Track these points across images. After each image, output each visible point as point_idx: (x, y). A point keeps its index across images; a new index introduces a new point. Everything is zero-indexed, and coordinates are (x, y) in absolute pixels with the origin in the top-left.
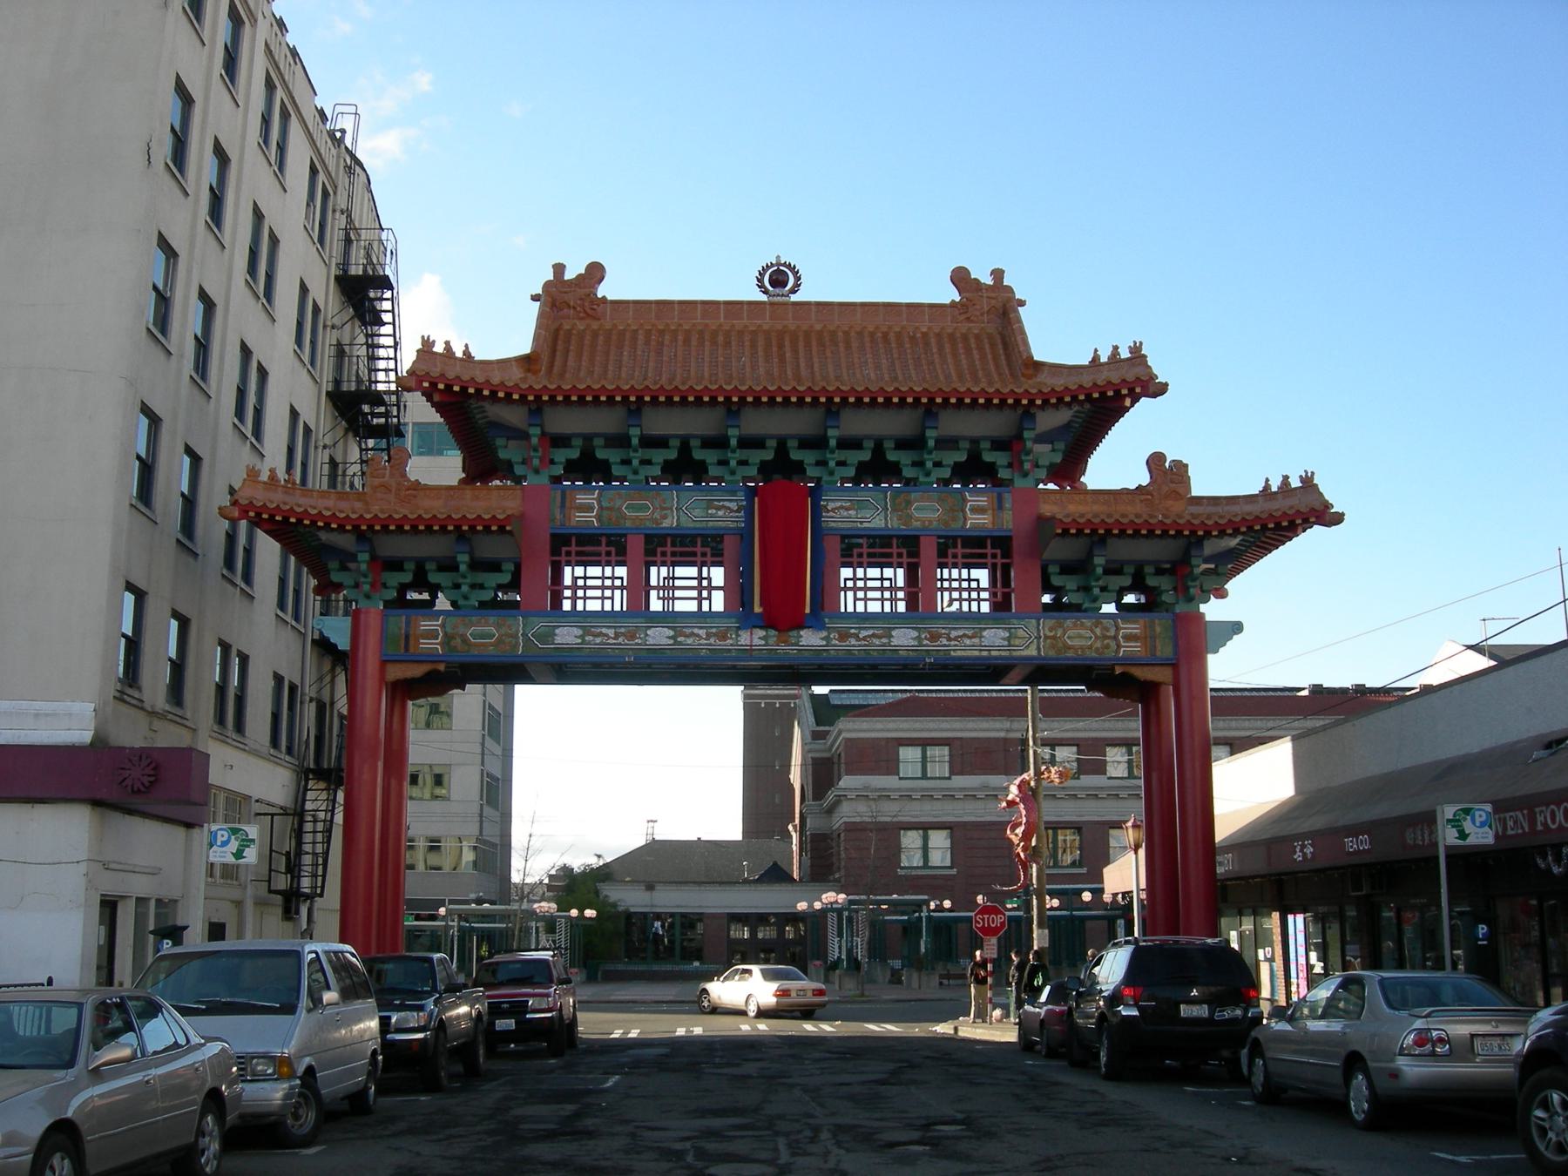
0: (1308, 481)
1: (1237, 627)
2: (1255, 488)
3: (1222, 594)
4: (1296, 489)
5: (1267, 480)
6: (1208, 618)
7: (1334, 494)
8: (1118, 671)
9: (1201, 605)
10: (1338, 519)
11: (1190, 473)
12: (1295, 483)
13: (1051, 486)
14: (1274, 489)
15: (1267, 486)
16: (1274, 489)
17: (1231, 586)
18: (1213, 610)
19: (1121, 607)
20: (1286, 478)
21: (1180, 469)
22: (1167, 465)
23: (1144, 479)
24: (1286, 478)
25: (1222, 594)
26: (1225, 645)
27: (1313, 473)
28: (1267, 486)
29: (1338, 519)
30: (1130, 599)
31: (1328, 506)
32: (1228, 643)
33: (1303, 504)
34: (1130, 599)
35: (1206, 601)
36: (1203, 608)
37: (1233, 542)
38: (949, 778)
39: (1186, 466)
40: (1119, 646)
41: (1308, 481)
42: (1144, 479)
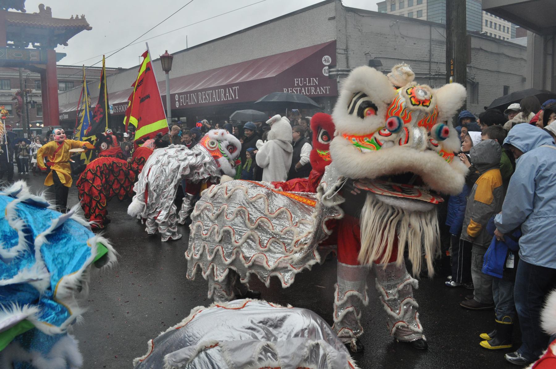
0: (83, 17)
1: (64, 55)
2: (69, 17)
3: (66, 45)
4: (80, 19)
5: (72, 16)
6: (56, 52)
7: (90, 21)
8: (30, 64)
9: (55, 49)
10: (90, 29)
11: (52, 11)
12: (80, 17)
13: (14, 10)
14: (74, 18)
15: (72, 17)
16: (74, 18)
17: (69, 42)
18: (59, 49)
19: (34, 46)
20: (77, 16)
21: (49, 9)
22: (45, 8)
23: (38, 11)
24: (77, 16)
25: (66, 45)
26: (61, 59)
27: (84, 15)
28: (72, 17)
29: (90, 29)
30: (36, 44)
31: (88, 25)
32: (62, 59)
33: (81, 24)
34: (36, 44)
35: (56, 46)
36: (55, 49)
37: (64, 31)
38: (10, 90)
39: (51, 9)
40: (30, 58)
41: (83, 17)
42: (38, 11)
